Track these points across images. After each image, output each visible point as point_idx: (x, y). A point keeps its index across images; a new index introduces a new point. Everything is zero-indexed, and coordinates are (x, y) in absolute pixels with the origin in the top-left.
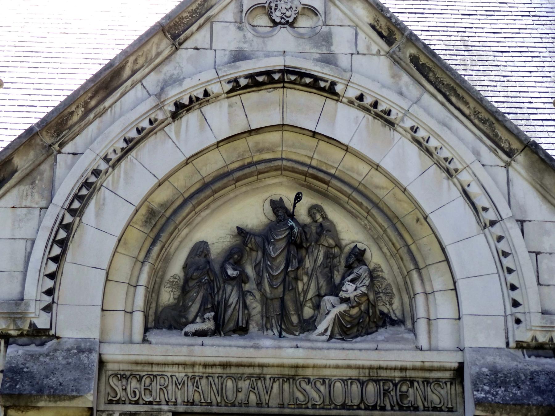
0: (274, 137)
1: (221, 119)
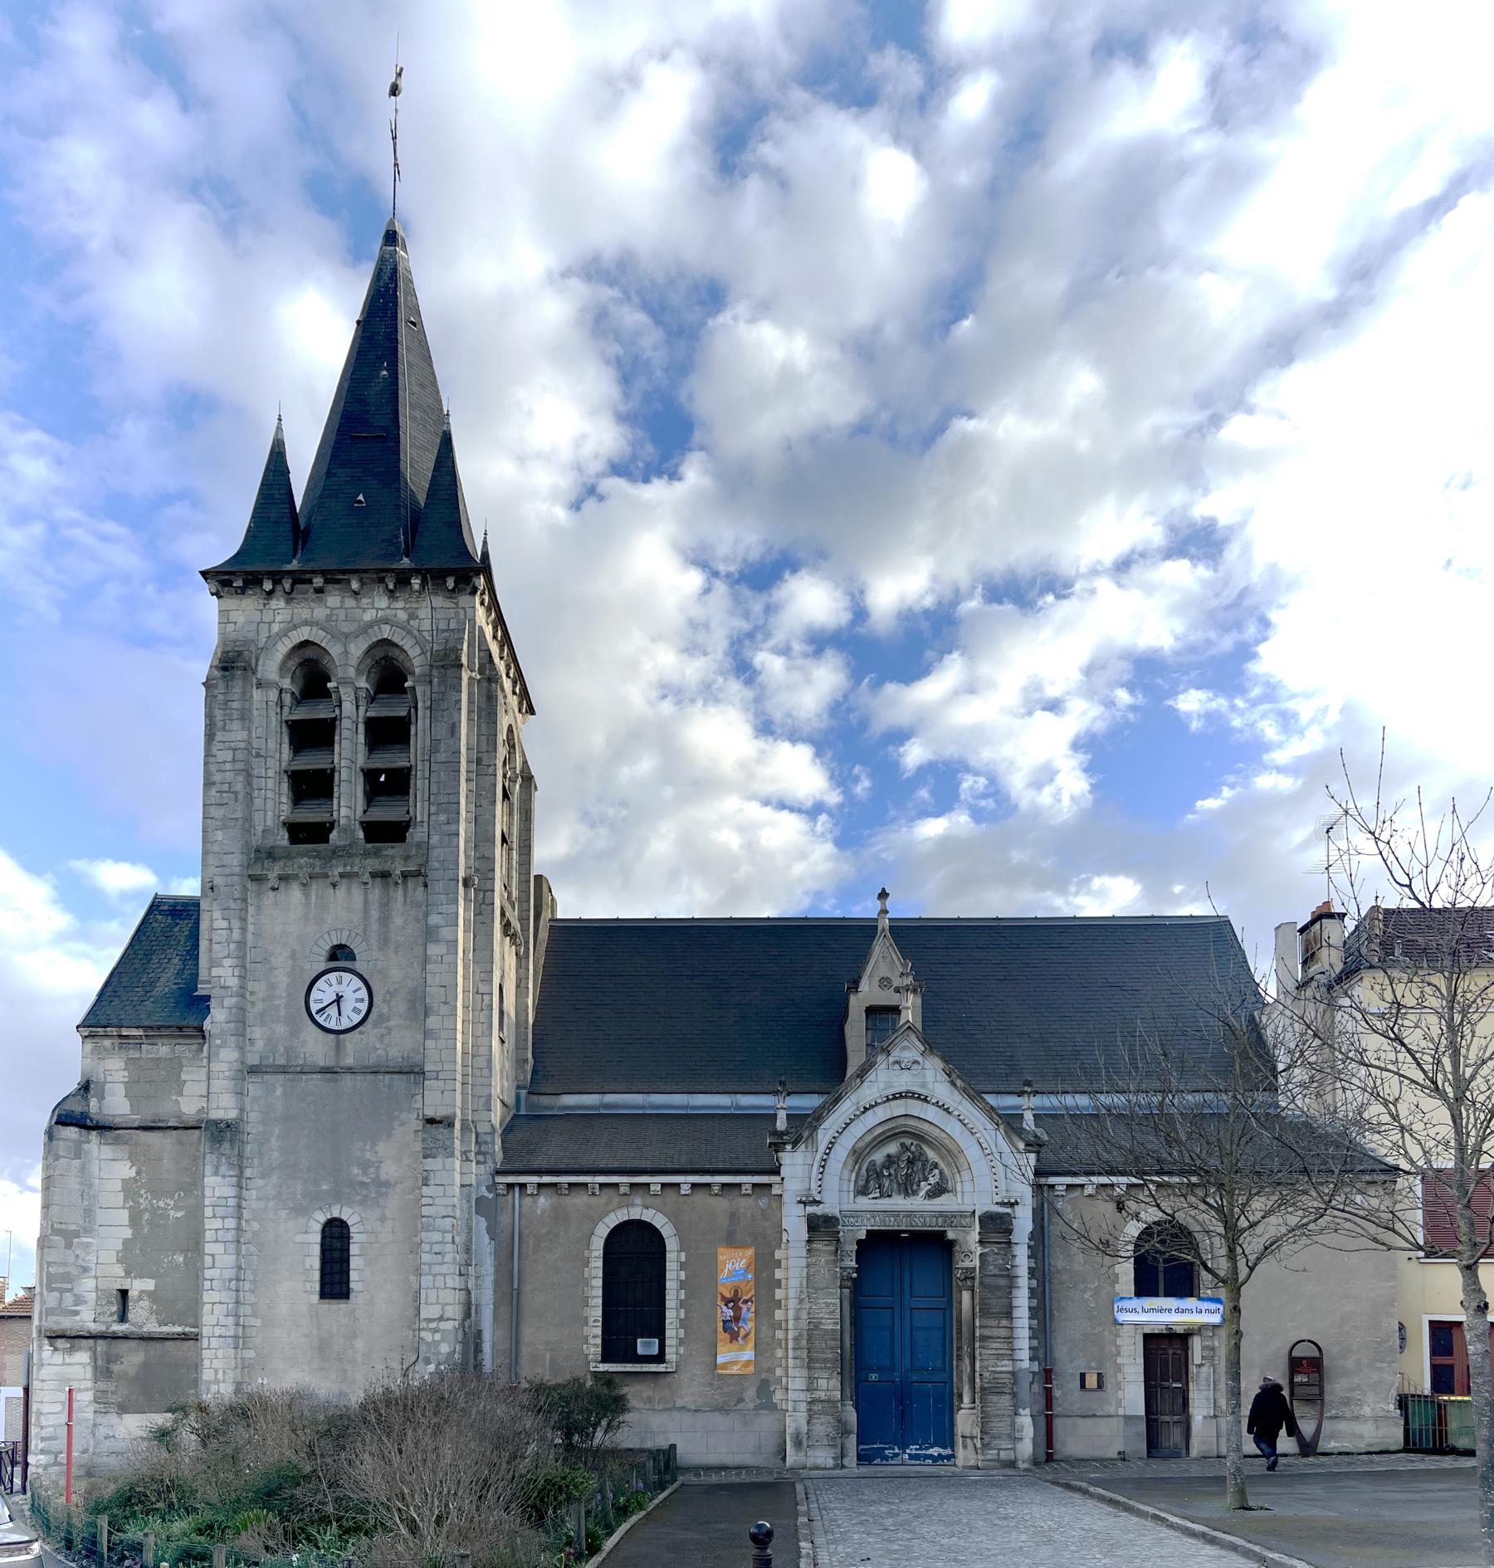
0: (901, 1121)
1: (882, 1113)
